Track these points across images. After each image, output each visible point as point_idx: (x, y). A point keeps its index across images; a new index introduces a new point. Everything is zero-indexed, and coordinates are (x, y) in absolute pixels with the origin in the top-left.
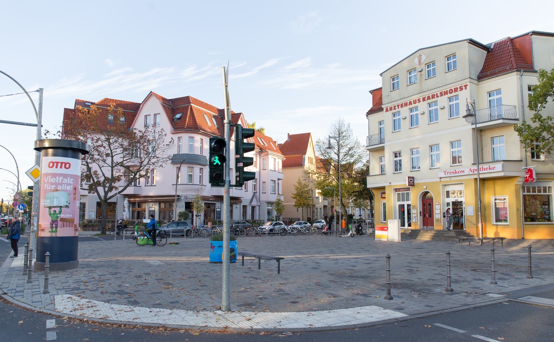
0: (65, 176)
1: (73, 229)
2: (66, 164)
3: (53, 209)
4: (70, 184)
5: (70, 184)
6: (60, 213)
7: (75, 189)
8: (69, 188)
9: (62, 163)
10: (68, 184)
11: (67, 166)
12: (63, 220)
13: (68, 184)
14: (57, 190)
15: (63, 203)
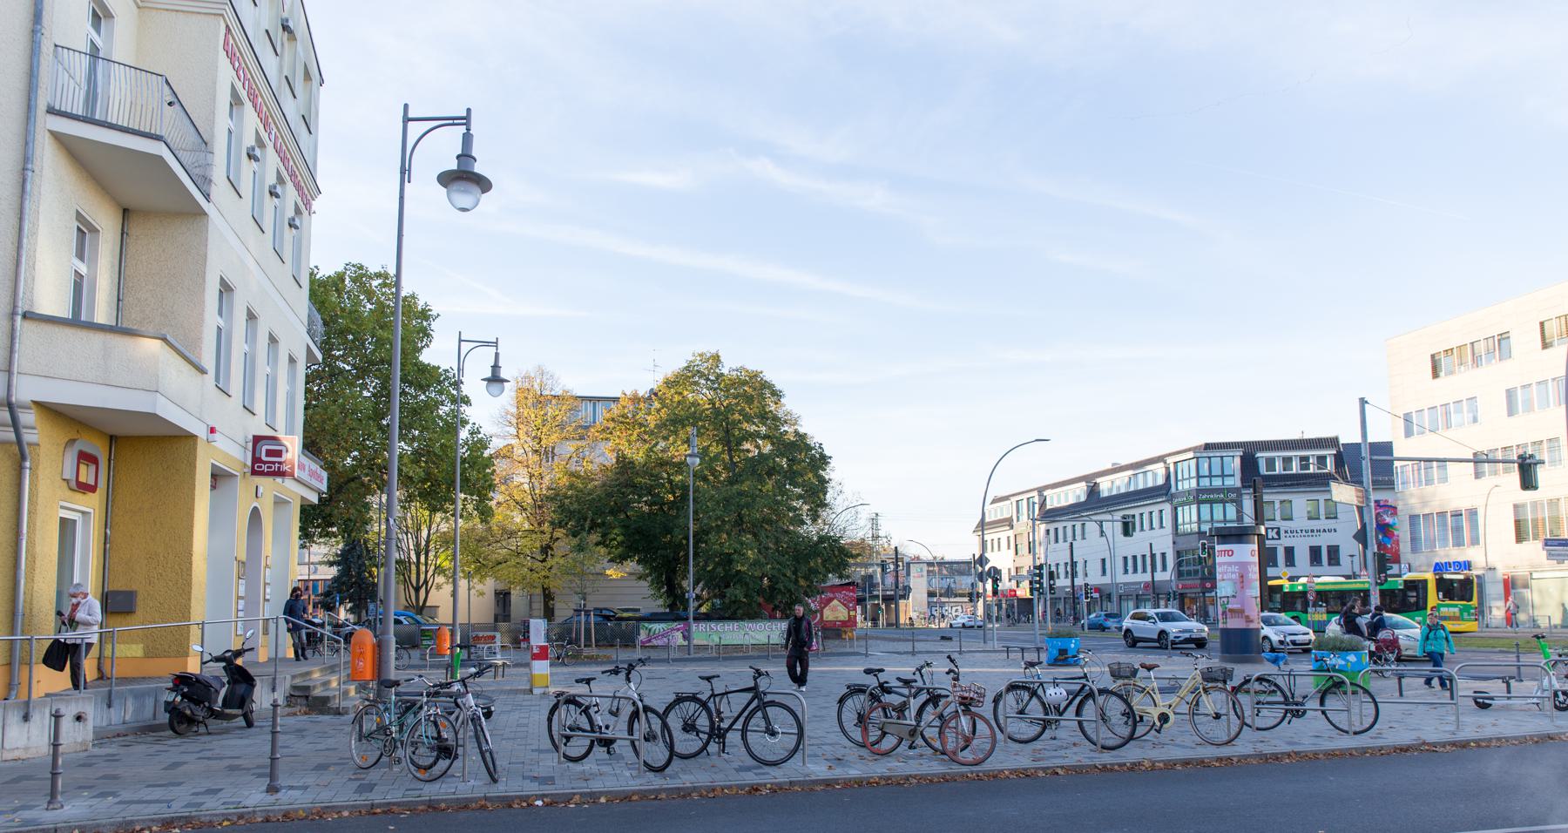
0: (1230, 564)
1: (1244, 620)
2: (1228, 551)
3: (1223, 599)
4: (1235, 573)
5: (1235, 573)
6: (1228, 604)
7: (1242, 577)
8: (1234, 576)
9: (1225, 551)
10: (1232, 573)
11: (1230, 553)
12: (1231, 610)
13: (1232, 573)
14: (1223, 580)
15: (1230, 593)
